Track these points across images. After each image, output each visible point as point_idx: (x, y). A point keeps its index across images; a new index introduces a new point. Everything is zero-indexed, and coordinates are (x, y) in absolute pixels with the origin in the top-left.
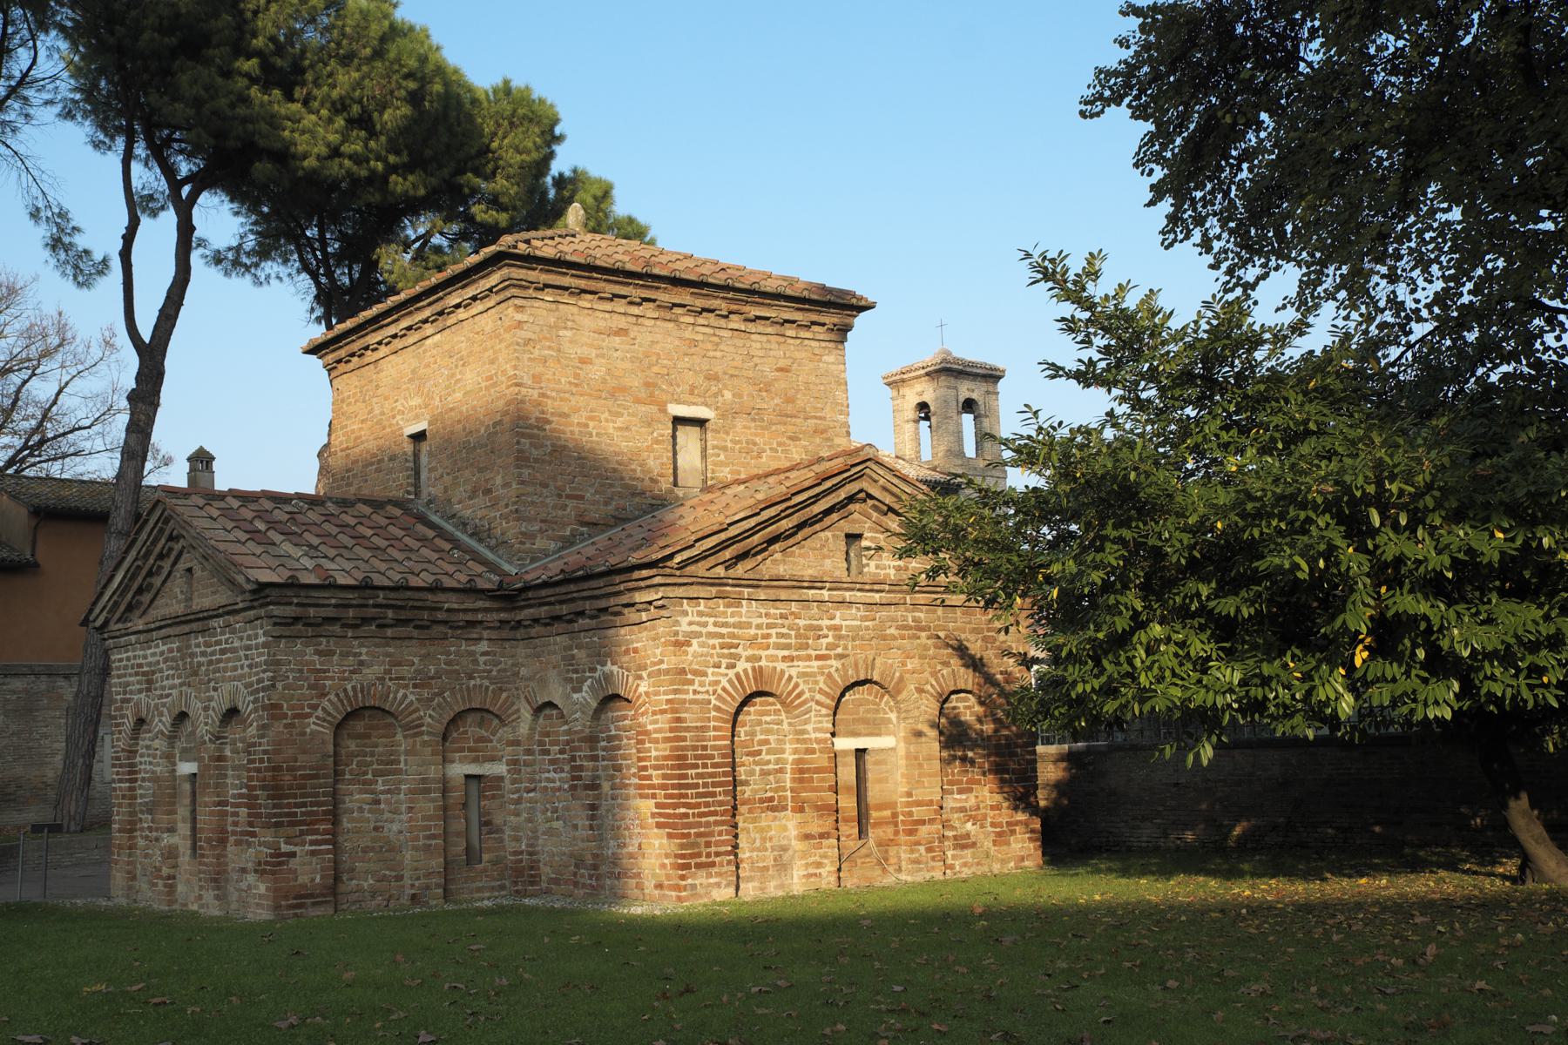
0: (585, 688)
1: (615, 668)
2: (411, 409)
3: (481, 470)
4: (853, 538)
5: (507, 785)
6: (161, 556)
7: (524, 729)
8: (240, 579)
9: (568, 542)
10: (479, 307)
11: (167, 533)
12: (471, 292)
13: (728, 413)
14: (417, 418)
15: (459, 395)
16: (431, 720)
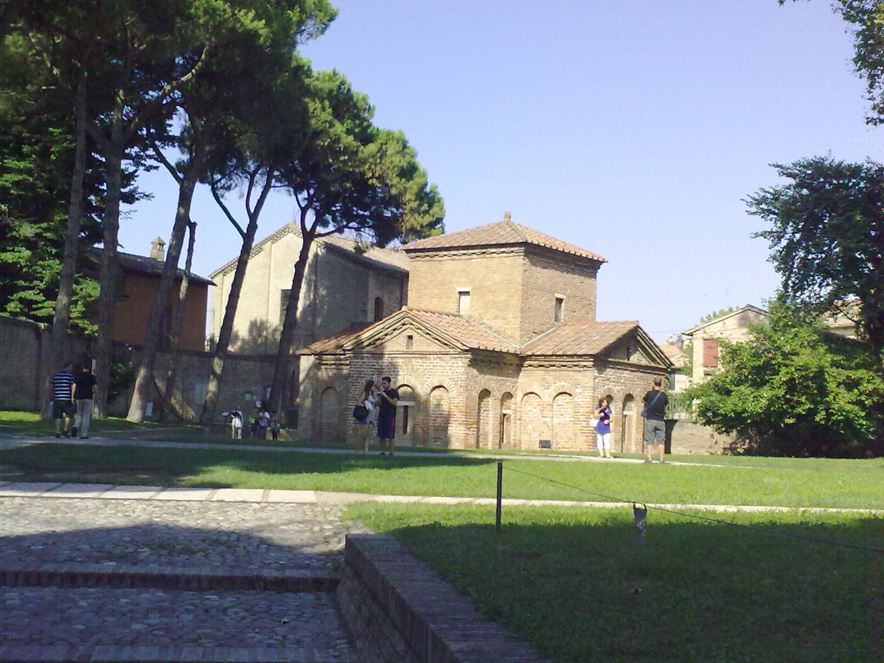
0: (551, 388)
1: (566, 384)
2: (461, 282)
3: (501, 311)
4: (628, 349)
5: (512, 417)
6: (395, 329)
7: (519, 399)
8: (459, 345)
9: (531, 339)
10: (505, 255)
11: (402, 322)
12: (503, 250)
13: (569, 297)
14: (464, 286)
15: (490, 283)
16: (499, 395)
